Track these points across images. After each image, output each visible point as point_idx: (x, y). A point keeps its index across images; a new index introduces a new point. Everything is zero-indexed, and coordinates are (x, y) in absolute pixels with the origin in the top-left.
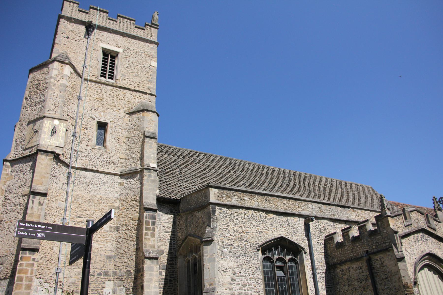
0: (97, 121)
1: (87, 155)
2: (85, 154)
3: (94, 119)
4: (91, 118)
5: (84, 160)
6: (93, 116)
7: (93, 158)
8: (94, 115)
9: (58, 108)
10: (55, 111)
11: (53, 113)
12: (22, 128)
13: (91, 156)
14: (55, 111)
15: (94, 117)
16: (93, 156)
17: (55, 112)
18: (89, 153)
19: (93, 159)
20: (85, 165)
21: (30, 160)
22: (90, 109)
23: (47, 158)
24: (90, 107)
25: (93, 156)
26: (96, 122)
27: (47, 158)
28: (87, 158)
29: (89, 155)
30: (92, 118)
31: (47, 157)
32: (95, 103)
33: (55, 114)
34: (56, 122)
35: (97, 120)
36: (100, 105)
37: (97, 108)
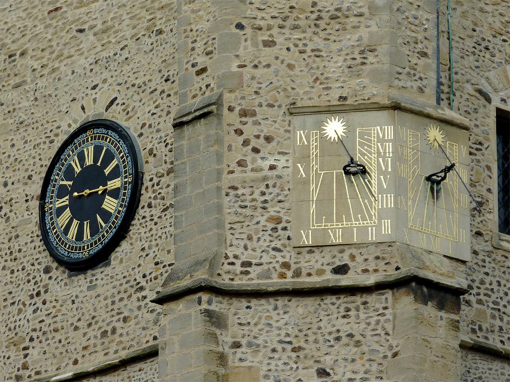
0: (498, 110)
1: (482, 282)
2: (474, 277)
3: (488, 100)
4: (478, 95)
5: (475, 305)
6: (483, 81)
7: (502, 294)
8: (487, 78)
9: (427, 60)
10: (421, 79)
11: (416, 85)
12: (250, 130)
13: (495, 286)
14: (421, 79)
15: (487, 89)
16: (499, 284)
17: (419, 83)
18: (486, 270)
19: (502, 303)
20: (480, 329)
21: (348, 310)
22: (470, 43)
23: (441, 318)
24: (469, 36)
25: (499, 284)
26: (493, 114)
27: (441, 318)
28: (482, 297)
29: (488, 279)
30: (480, 92)
31: (443, 314)
32: (482, 10)
33: (421, 90)
34: (435, 133)
35: (496, 102)
36: (498, 25)
37: (491, 38)
